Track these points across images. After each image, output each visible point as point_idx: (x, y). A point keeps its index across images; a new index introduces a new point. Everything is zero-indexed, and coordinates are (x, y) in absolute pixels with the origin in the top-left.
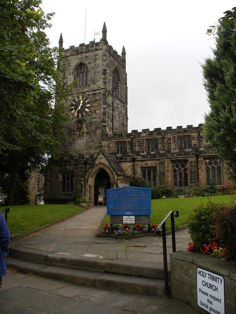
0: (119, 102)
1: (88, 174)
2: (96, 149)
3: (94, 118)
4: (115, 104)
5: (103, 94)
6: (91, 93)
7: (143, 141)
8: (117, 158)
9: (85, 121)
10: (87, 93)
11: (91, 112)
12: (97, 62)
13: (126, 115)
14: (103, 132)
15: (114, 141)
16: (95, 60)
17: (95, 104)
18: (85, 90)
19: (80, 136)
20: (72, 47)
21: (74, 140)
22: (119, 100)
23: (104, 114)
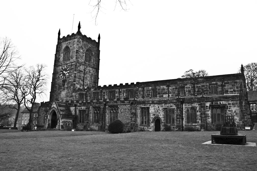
0: (91, 69)
1: (48, 113)
2: (70, 98)
4: (87, 70)
5: (75, 65)
6: (70, 64)
7: (92, 94)
8: (69, 104)
9: (66, 81)
10: (68, 64)
12: (75, 46)
14: (73, 87)
15: (78, 93)
16: (74, 44)
17: (72, 71)
18: (68, 62)
19: (63, 90)
20: (64, 37)
21: (61, 92)
22: (91, 67)
23: (75, 77)
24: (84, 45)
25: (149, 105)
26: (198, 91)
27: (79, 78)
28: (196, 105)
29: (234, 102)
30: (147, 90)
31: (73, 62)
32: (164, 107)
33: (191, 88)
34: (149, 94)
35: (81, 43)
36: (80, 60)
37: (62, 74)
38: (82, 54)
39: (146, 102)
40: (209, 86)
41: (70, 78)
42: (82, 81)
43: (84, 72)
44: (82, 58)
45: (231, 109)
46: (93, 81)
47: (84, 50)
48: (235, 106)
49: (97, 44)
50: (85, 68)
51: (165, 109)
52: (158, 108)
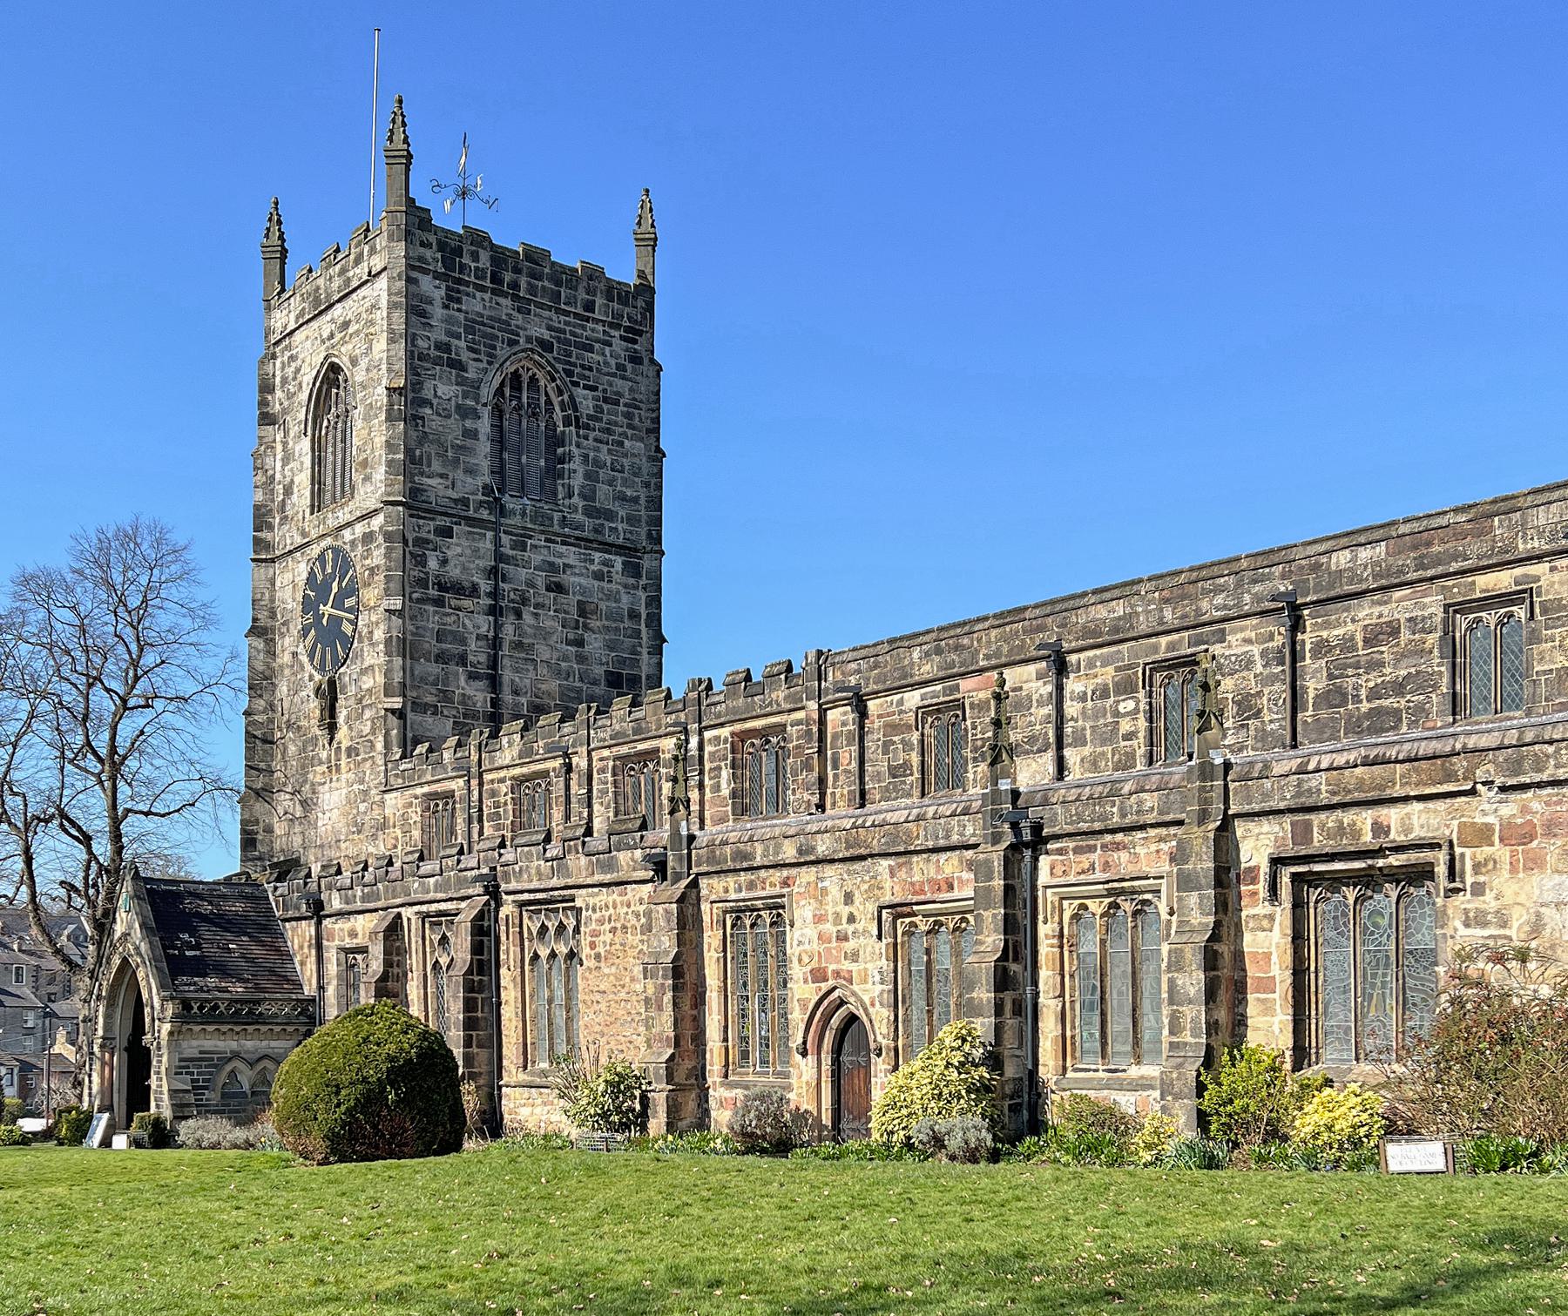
0: (571, 555)
13: (655, 620)
24: (469, 330)
25: (777, 876)
26: (1334, 696)
27: (441, 658)
28: (1147, 857)
29: (1525, 810)
30: (892, 728)
32: (887, 899)
33: (1259, 668)
34: (906, 765)
35: (438, 312)
36: (433, 482)
38: (452, 429)
39: (759, 848)
40: (1448, 628)
42: (472, 676)
43: (494, 594)
44: (456, 461)
45: (1488, 902)
46: (599, 671)
47: (476, 385)
48: (1535, 863)
49: (635, 306)
50: (500, 557)
51: (899, 910)
52: (845, 911)
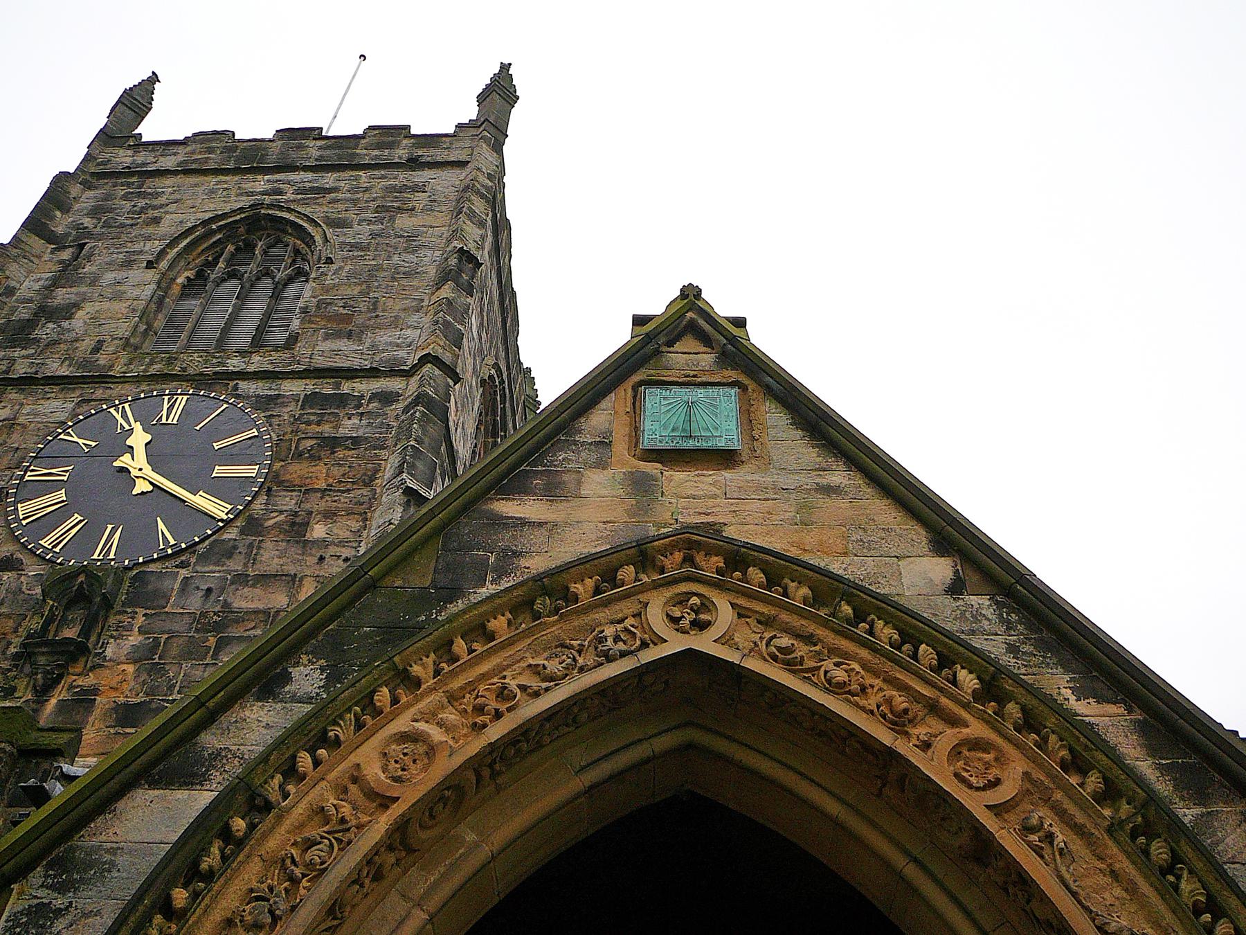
3: (264, 579)
11: (253, 526)
31: (373, 373)
37: (62, 495)
41: (251, 556)
